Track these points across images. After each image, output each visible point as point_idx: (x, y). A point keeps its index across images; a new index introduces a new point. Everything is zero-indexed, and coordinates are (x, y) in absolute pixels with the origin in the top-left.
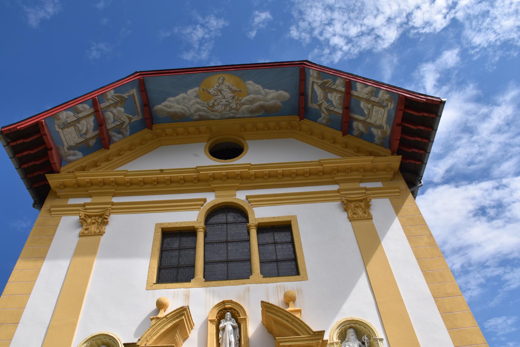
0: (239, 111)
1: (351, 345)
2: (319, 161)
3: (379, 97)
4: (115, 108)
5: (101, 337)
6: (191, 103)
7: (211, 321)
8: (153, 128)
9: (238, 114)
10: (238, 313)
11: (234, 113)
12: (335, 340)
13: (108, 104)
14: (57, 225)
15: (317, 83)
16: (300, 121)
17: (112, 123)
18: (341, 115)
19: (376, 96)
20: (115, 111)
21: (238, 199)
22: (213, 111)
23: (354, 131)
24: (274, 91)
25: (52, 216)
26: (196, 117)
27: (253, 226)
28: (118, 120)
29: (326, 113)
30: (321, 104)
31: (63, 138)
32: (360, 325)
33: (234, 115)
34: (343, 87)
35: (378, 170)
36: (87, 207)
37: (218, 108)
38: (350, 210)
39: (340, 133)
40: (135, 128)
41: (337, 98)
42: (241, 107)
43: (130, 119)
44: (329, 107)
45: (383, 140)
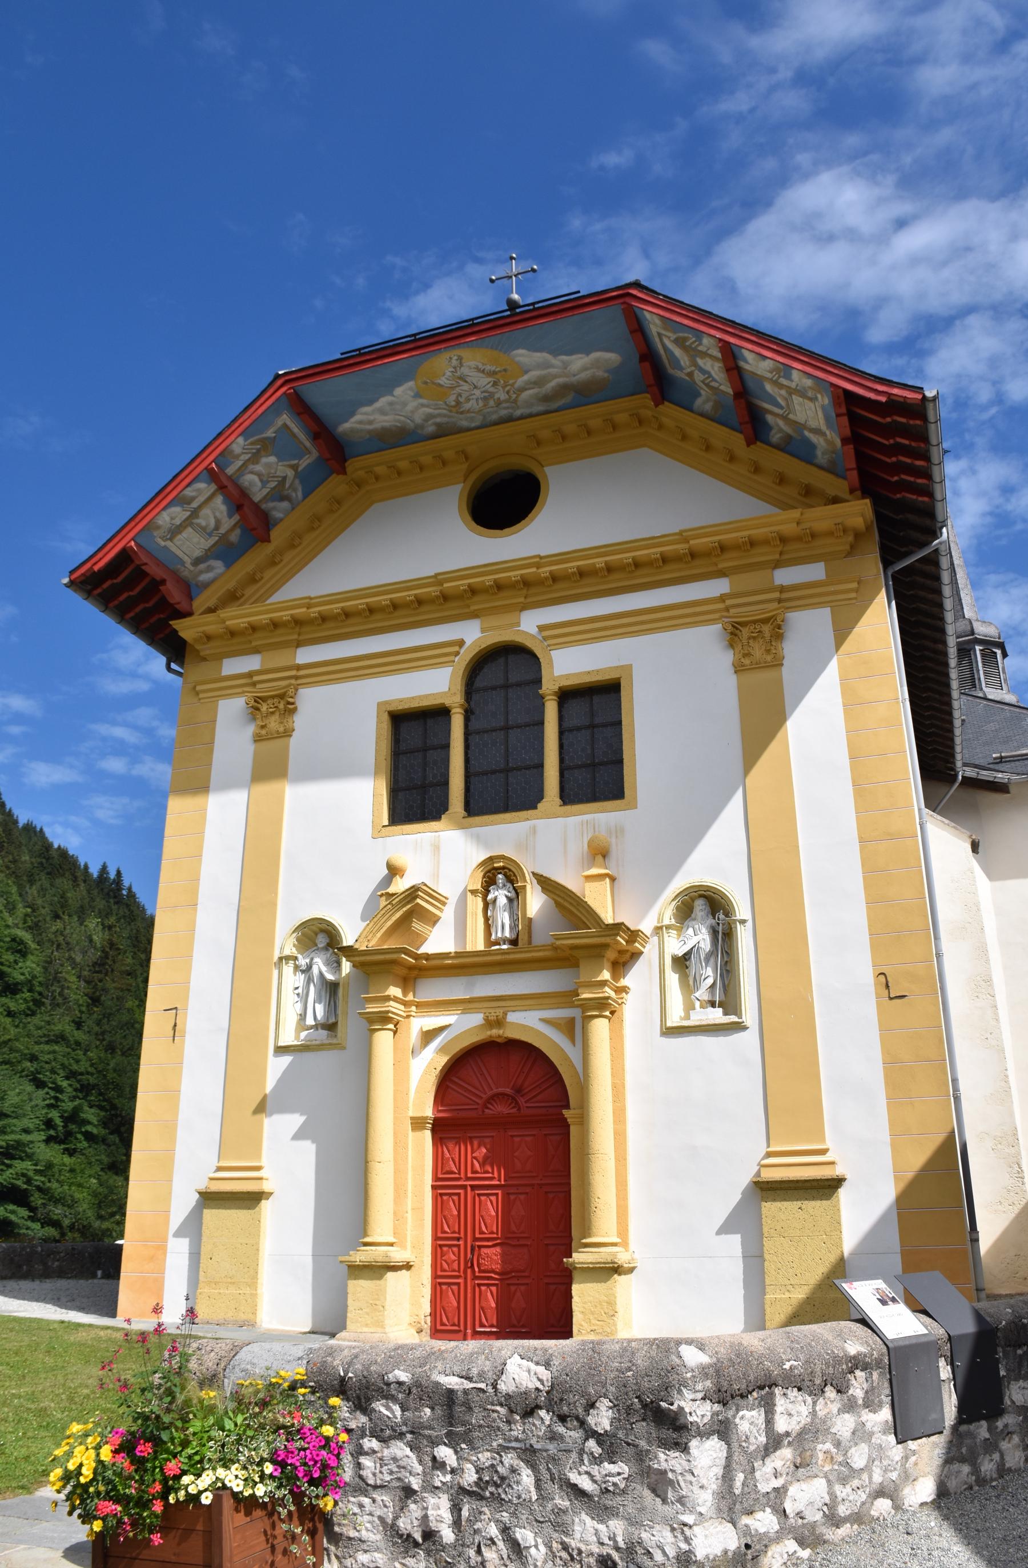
0: (519, 403)
1: (697, 926)
2: (681, 533)
4: (257, 463)
5: (315, 923)
7: (474, 892)
9: (518, 408)
11: (508, 408)
12: (668, 919)
13: (240, 463)
14: (214, 721)
15: (669, 338)
16: (658, 409)
17: (260, 490)
20: (258, 468)
21: (523, 631)
22: (462, 413)
23: (773, 432)
24: (580, 356)
25: (202, 701)
26: (431, 429)
27: (550, 695)
33: (510, 411)
35: (813, 535)
36: (256, 678)
38: (740, 646)
40: (310, 481)
41: (716, 369)
42: (518, 395)
43: (294, 468)
45: (834, 455)
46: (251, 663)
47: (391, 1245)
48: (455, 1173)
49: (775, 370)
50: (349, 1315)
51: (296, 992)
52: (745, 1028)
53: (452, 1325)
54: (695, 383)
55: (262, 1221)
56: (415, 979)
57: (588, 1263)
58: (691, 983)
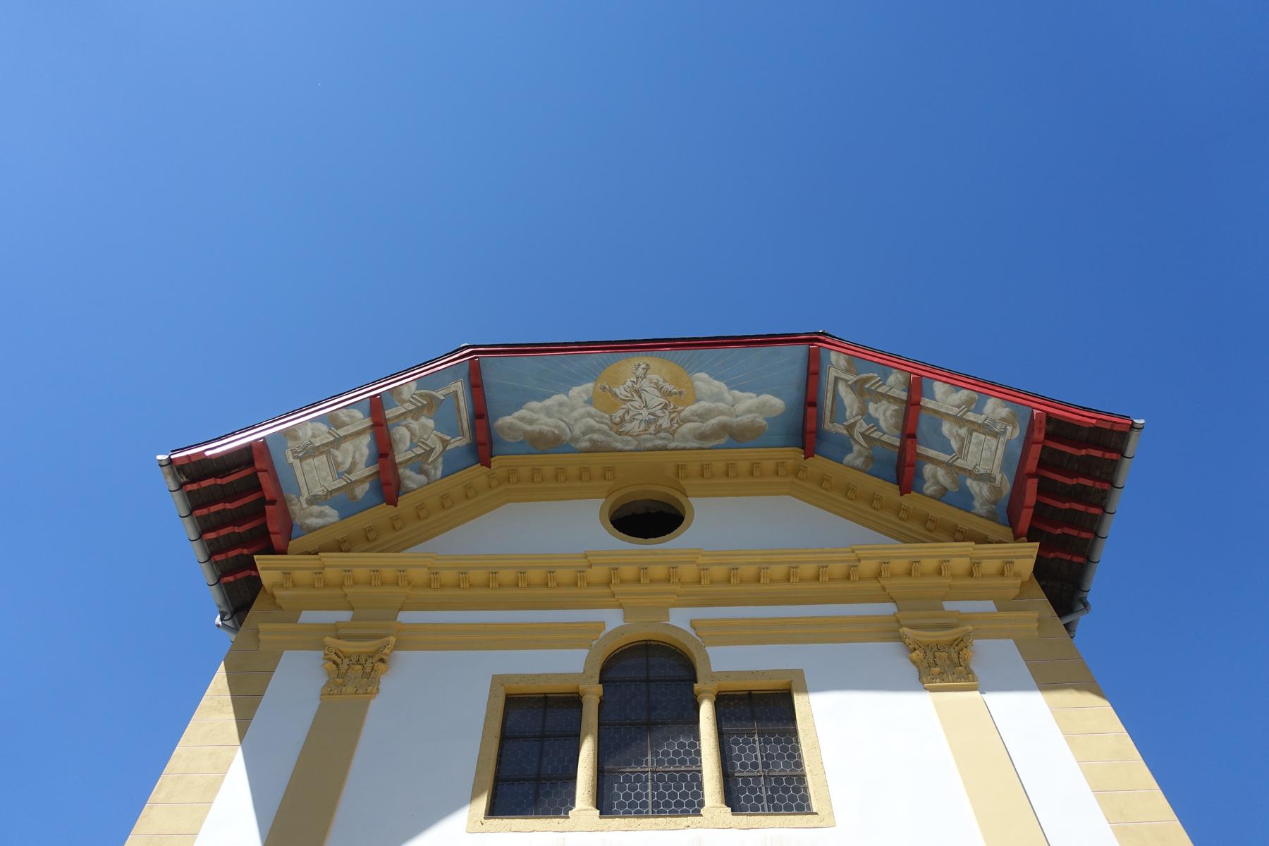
0: (675, 436)
3: (986, 413)
6: (576, 414)
8: (492, 464)
9: (673, 441)
13: (403, 410)
15: (846, 381)
18: (897, 450)
19: (979, 410)
20: (415, 425)
22: (620, 434)
24: (752, 394)
26: (585, 444)
28: (419, 444)
29: (863, 443)
30: (854, 424)
31: (301, 479)
33: (666, 442)
34: (903, 390)
36: (341, 632)
41: (888, 413)
42: (680, 426)
43: (445, 443)
45: (994, 507)
49: (968, 403)
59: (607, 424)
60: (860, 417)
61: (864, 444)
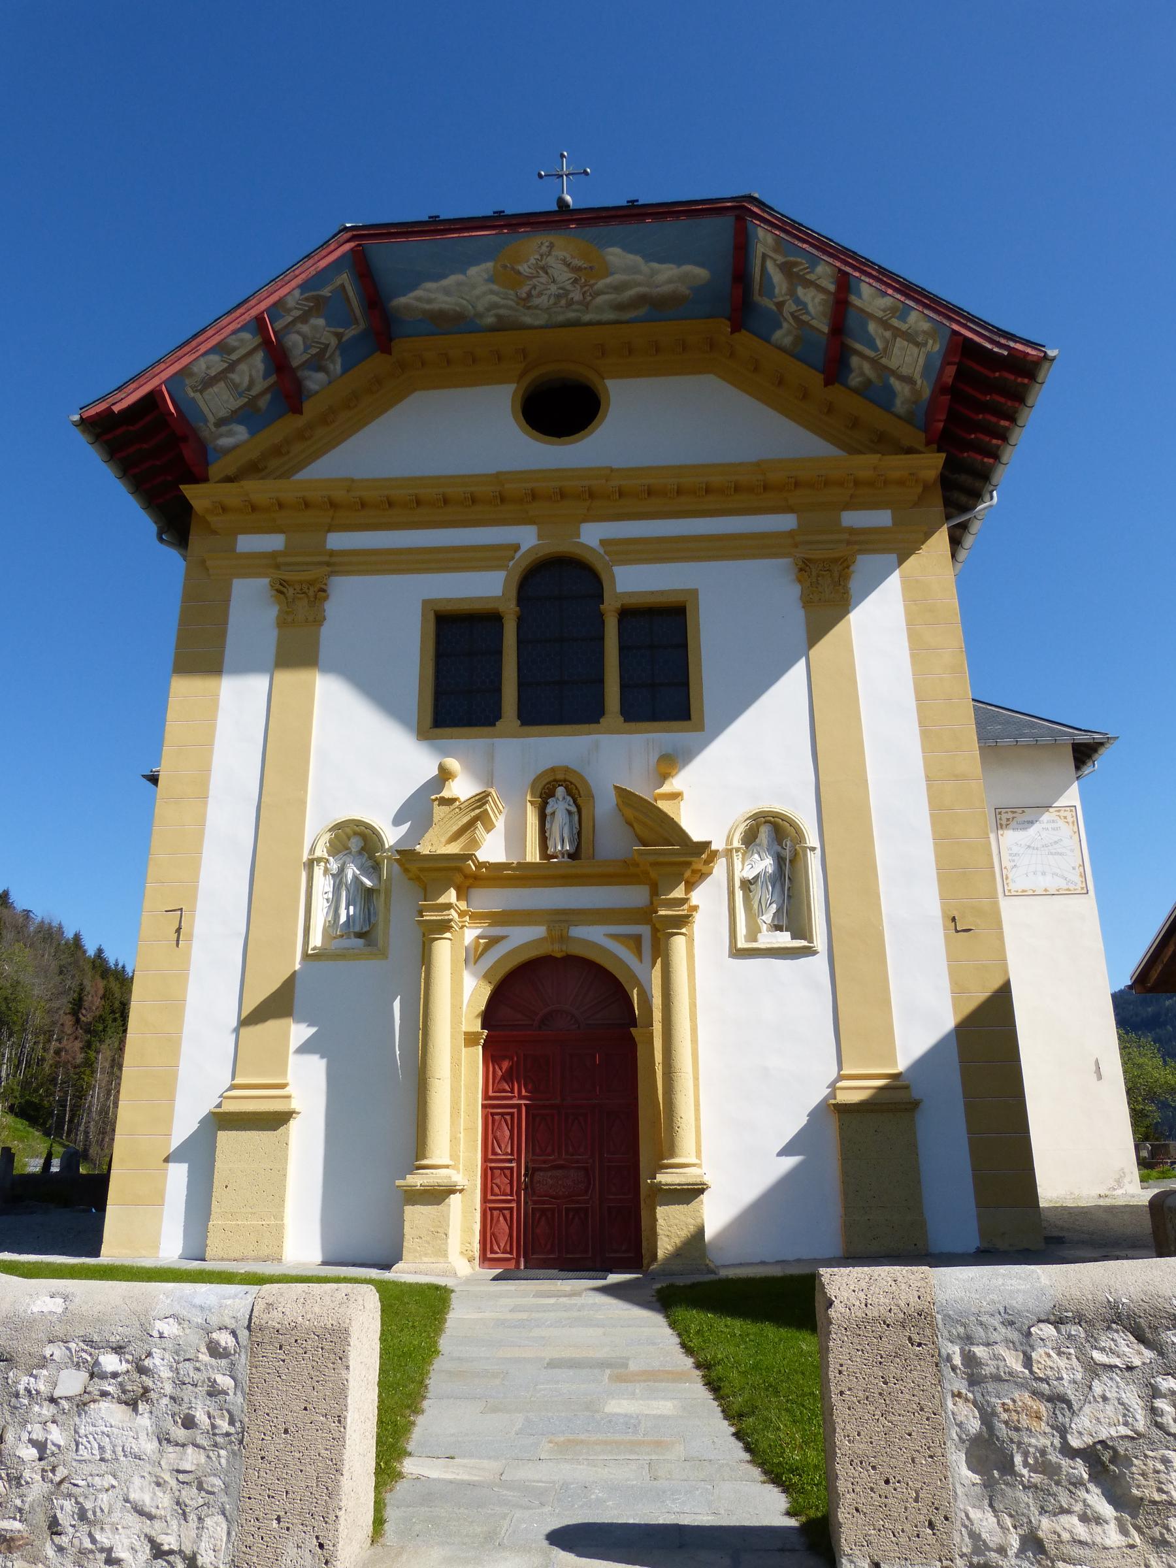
6: (477, 292)
10: (577, 788)
11: (577, 311)
12: (736, 843)
13: (290, 319)
15: (775, 260)
19: (903, 318)
20: (305, 328)
22: (529, 308)
23: (853, 375)
24: (671, 266)
26: (490, 320)
29: (791, 321)
32: (783, 820)
33: (579, 314)
34: (832, 283)
36: (280, 560)
37: (543, 301)
39: (819, 378)
40: (352, 354)
41: (817, 300)
42: (594, 298)
43: (339, 336)
44: (799, 313)
45: (914, 406)
46: (274, 542)
47: (447, 1167)
48: (507, 1092)
49: (893, 310)
50: (405, 1244)
51: (326, 896)
52: (815, 953)
53: (503, 1253)
54: (781, 313)
55: (290, 1144)
56: (468, 887)
57: (676, 1185)
58: (756, 906)
59: (512, 300)
60: (788, 297)
61: (793, 324)
